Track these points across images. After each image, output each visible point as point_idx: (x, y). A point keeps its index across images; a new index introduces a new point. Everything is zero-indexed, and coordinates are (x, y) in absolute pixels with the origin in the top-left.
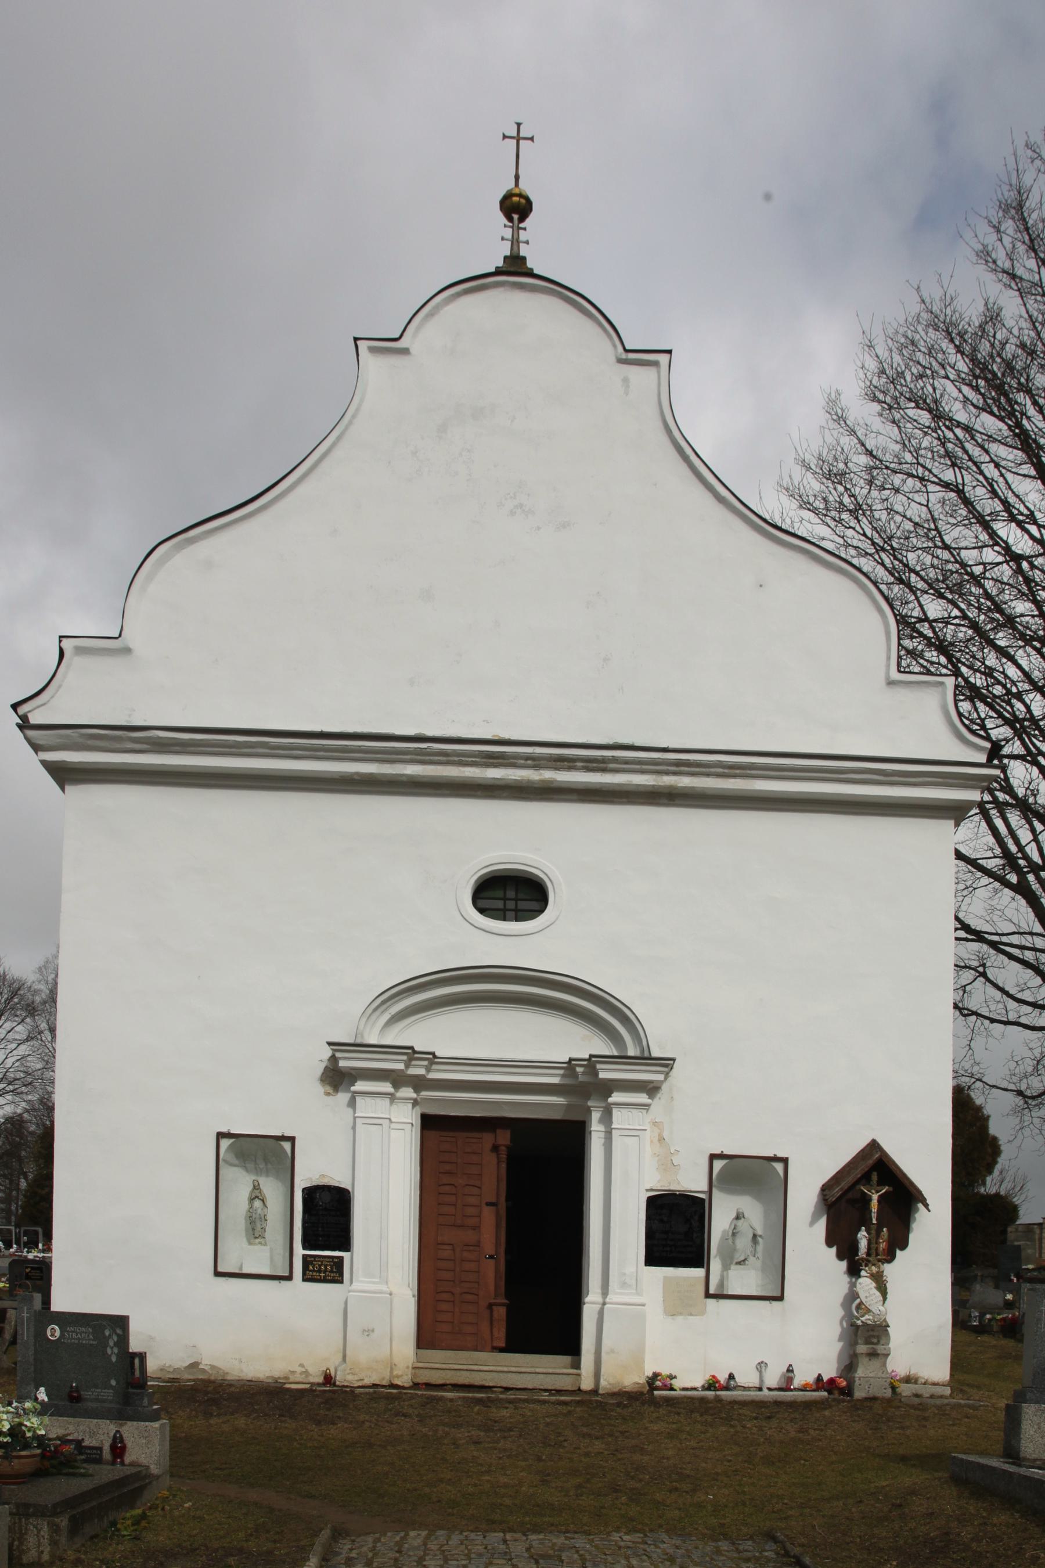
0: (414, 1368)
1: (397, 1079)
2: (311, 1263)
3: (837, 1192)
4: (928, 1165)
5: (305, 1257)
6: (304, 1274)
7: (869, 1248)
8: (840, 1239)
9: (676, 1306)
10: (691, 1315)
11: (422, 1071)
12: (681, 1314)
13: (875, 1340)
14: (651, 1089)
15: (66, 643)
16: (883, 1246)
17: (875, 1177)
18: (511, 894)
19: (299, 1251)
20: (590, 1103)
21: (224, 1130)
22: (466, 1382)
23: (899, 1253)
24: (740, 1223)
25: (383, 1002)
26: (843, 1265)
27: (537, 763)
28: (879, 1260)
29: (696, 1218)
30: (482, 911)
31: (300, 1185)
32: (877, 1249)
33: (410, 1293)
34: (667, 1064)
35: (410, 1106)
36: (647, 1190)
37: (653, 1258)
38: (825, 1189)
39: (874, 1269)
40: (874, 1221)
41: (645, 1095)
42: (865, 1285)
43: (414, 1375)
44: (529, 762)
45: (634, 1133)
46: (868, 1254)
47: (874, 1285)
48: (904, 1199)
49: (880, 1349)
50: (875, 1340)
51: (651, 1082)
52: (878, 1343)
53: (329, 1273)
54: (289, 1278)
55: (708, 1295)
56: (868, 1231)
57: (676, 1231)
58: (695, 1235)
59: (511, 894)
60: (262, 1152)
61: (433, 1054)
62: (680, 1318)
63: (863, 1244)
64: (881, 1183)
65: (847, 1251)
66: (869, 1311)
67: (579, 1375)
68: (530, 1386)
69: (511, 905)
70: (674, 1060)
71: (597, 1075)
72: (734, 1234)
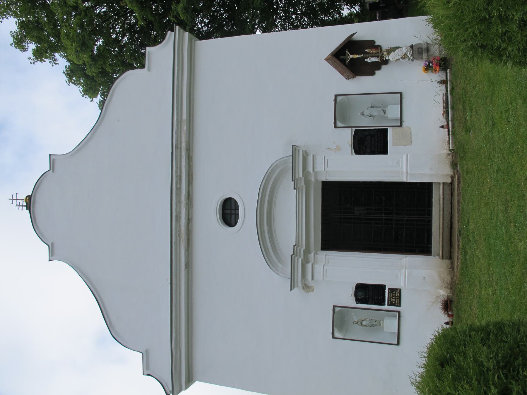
0: (443, 258)
1: (305, 261)
2: (391, 302)
3: (348, 72)
4: (335, 36)
5: (389, 305)
6: (397, 306)
7: (375, 57)
8: (370, 70)
9: (407, 140)
10: (411, 133)
11: (302, 250)
12: (411, 138)
13: (420, 50)
14: (305, 155)
15: (146, 373)
16: (374, 51)
17: (342, 57)
18: (229, 212)
19: (386, 307)
20: (313, 180)
21: (331, 335)
22: (448, 235)
23: (377, 44)
24: (365, 114)
26: (383, 67)
27: (179, 202)
28: (381, 52)
29: (364, 133)
30: (236, 223)
31: (353, 304)
32: (376, 53)
33: (405, 259)
34: (294, 148)
36: (352, 155)
37: (384, 151)
38: (348, 78)
39: (385, 53)
40: (362, 55)
41: (309, 157)
42: (392, 57)
43: (446, 258)
44: (178, 205)
45: (326, 162)
46: (378, 57)
47: (393, 53)
48: (350, 45)
49: (424, 47)
50: (420, 50)
51: (303, 155)
52: (422, 49)
53: (396, 296)
54: (399, 312)
55: (401, 126)
56: (367, 58)
57: (371, 142)
58: (372, 133)
59: (229, 212)
60: (340, 318)
61: (294, 246)
63: (373, 60)
64: (345, 54)
65: (377, 66)
66: (406, 54)
67: (444, 183)
68: (450, 206)
69: (233, 212)
70: (293, 146)
72: (371, 116)
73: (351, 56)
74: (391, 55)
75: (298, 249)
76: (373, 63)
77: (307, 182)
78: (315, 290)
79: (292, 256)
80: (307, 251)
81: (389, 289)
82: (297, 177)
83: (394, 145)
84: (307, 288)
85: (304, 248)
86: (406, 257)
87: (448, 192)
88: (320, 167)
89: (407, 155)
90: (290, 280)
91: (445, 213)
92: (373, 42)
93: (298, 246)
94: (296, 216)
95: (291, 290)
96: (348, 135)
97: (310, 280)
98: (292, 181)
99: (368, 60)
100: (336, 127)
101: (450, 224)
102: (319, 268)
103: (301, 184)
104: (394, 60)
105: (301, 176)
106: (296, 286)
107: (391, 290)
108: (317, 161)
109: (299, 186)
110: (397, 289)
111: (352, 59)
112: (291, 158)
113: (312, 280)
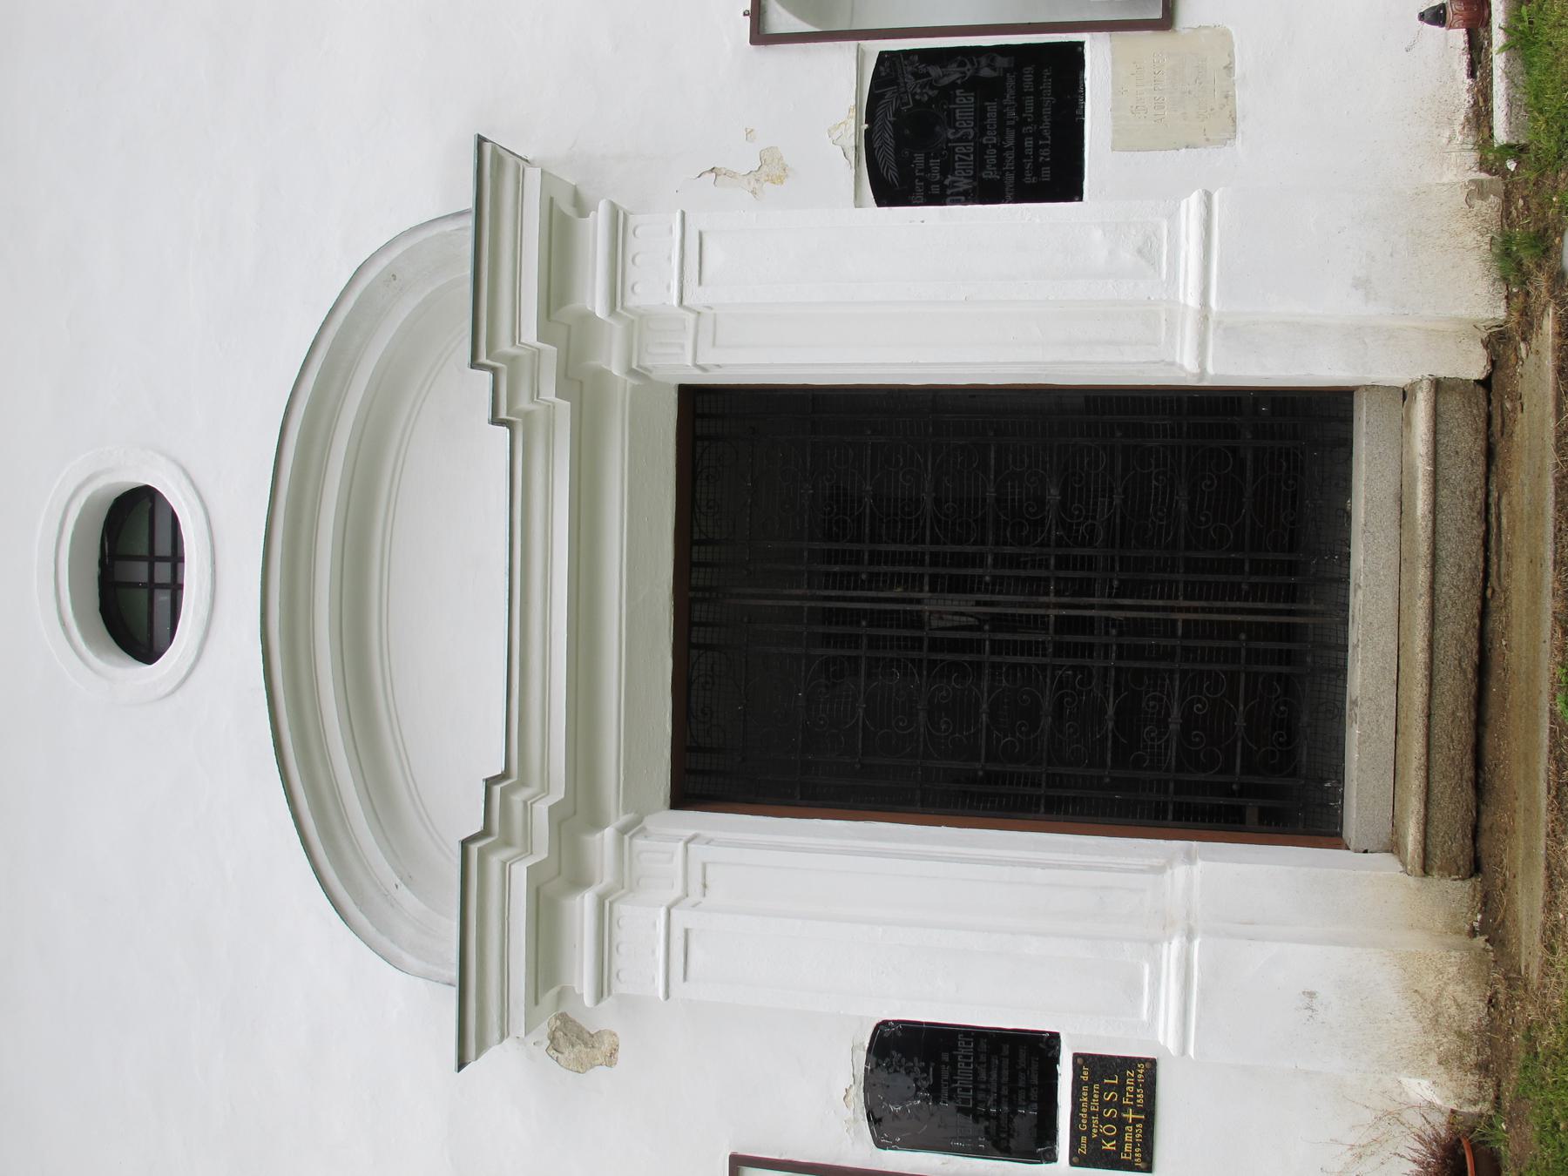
0: (1426, 870)
2: (1095, 1144)
10: (1229, 68)
11: (541, 810)
12: (1228, 97)
20: (616, 369)
22: (1465, 716)
25: (361, 902)
29: (935, 71)
33: (1180, 871)
35: (640, 843)
36: (858, 202)
37: (1058, 178)
43: (1449, 870)
58: (986, 72)
61: (490, 783)
62: (1242, 98)
68: (1479, 530)
71: (537, 354)
75: (517, 799)
77: (582, 385)
78: (620, 1055)
79: (465, 844)
80: (579, 814)
81: (1081, 1061)
82: (505, 346)
83: (1123, 142)
84: (572, 1040)
85: (558, 793)
86: (1190, 859)
87: (1466, 441)
88: (654, 285)
89: (1208, 196)
90: (454, 992)
91: (1444, 577)
93: (524, 782)
94: (515, 597)
95: (461, 1065)
96: (834, 84)
97: (588, 1000)
98: (475, 364)
100: (760, 35)
101: (1473, 645)
102: (642, 926)
103: (535, 393)
105: (530, 334)
106: (494, 1032)
107: (1094, 1068)
108: (635, 245)
109: (524, 404)
110: (1130, 1063)
112: (469, 222)
113: (600, 995)
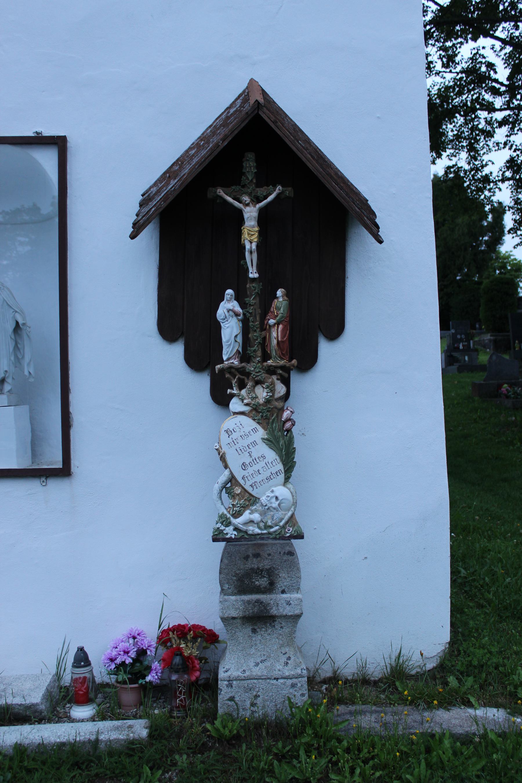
17: (250, 166)
28: (271, 371)
32: (264, 343)
40: (253, 274)
46: (244, 356)
47: (261, 433)
48: (321, 214)
63: (230, 331)
64: (265, 180)
66: (251, 500)
73: (251, 214)
74: (248, 423)
76: (216, 328)
92: (335, 329)
99: (228, 307)
104: (224, 436)
111: (239, 218)
